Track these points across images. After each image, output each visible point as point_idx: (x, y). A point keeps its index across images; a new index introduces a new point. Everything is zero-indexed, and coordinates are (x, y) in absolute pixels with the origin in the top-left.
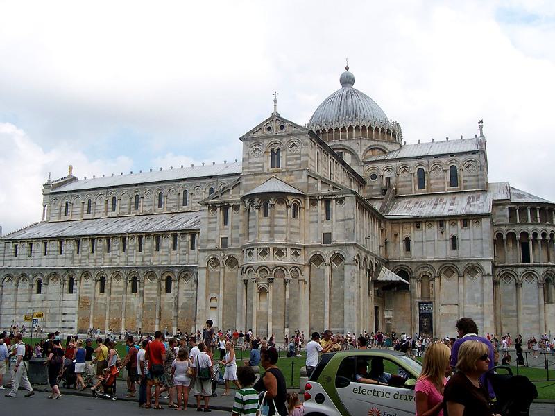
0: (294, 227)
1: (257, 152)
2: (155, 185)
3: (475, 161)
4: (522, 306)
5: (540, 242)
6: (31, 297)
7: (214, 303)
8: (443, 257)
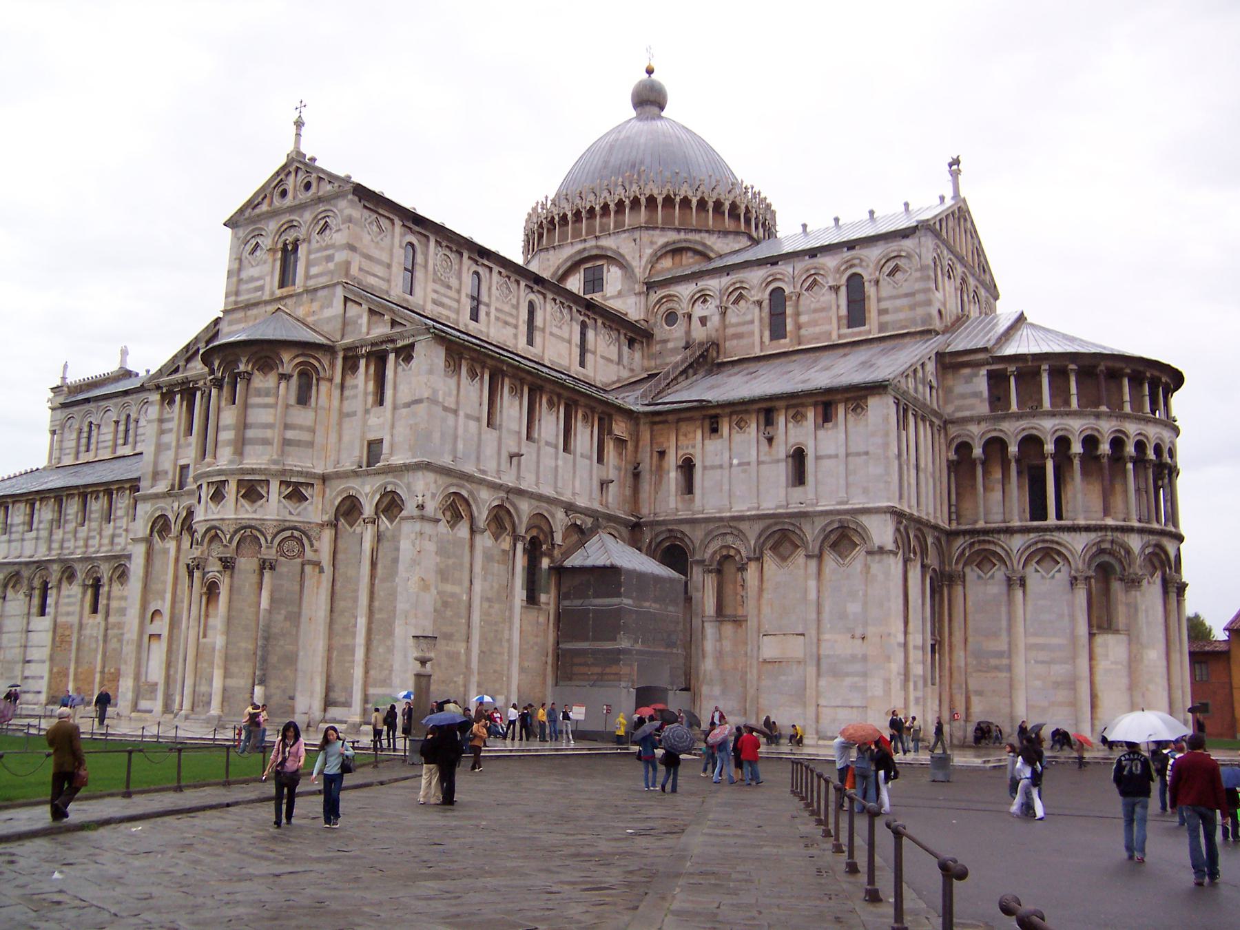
0: (301, 428)
1: (258, 253)
3: (909, 257)
4: (1021, 642)
5: (1077, 462)
8: (770, 504)
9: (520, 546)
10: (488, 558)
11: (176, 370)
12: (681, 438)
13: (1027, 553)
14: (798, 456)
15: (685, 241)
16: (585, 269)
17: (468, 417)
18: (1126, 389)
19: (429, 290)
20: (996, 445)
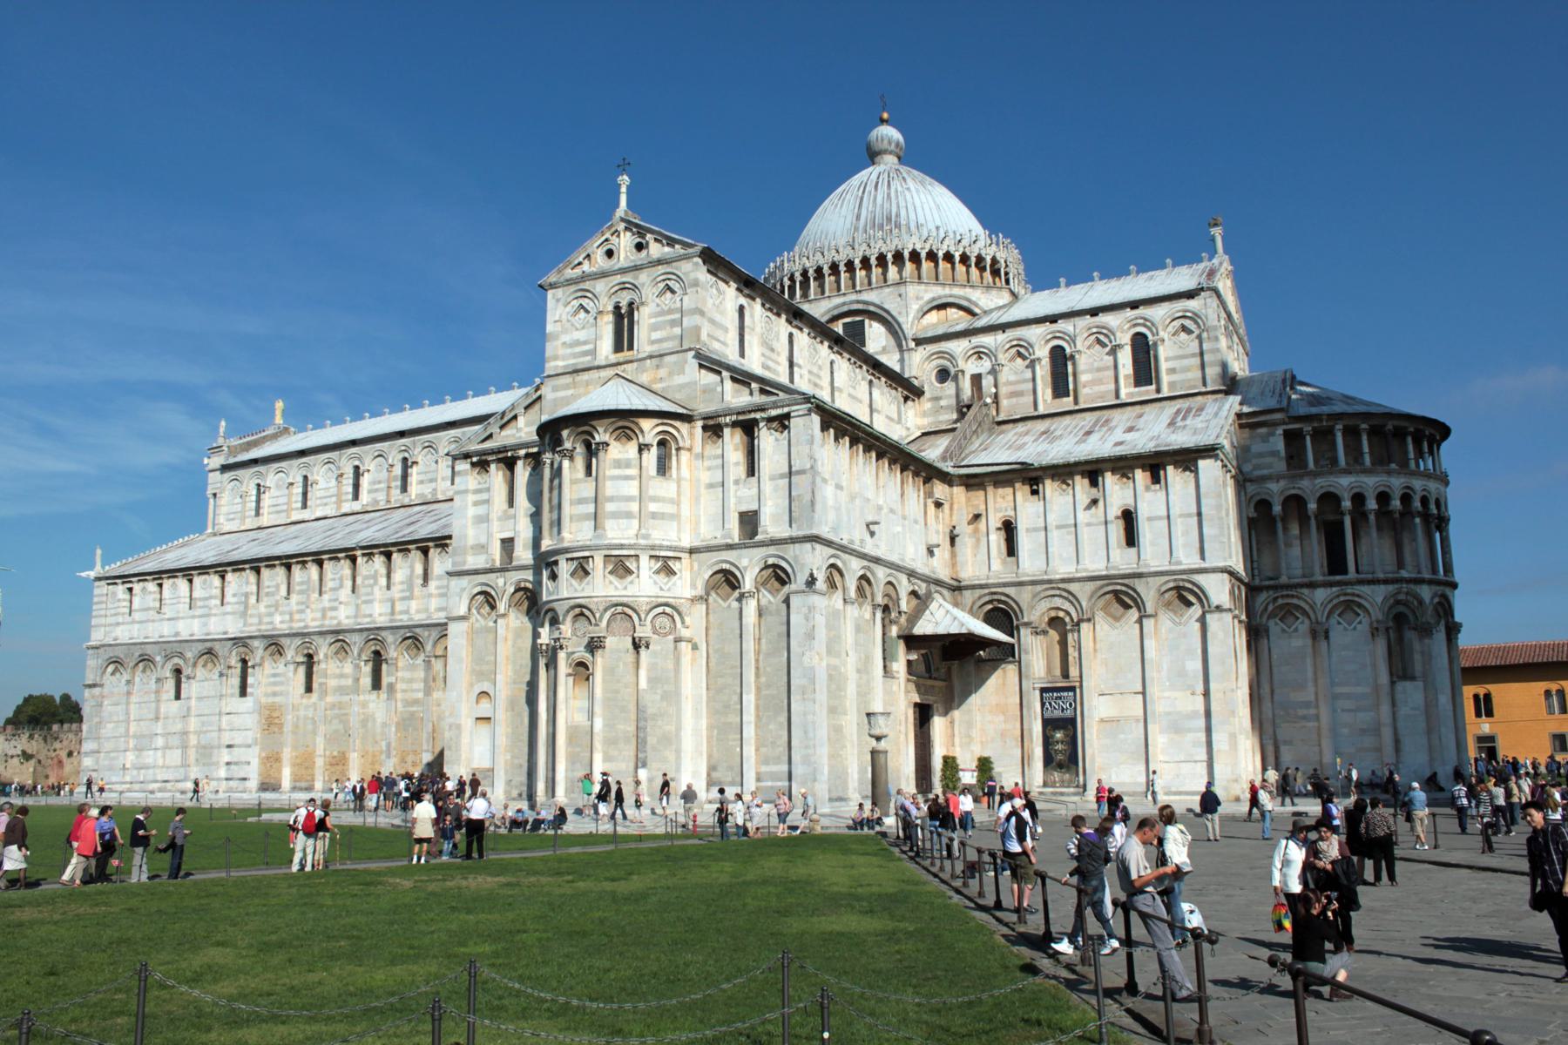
5: (1372, 517)
6: (157, 710)
7: (485, 708)
9: (879, 615)
10: (858, 629)
11: (490, 436)
13: (1330, 606)
14: (1129, 518)
16: (844, 324)
18: (1411, 447)
20: (1295, 503)
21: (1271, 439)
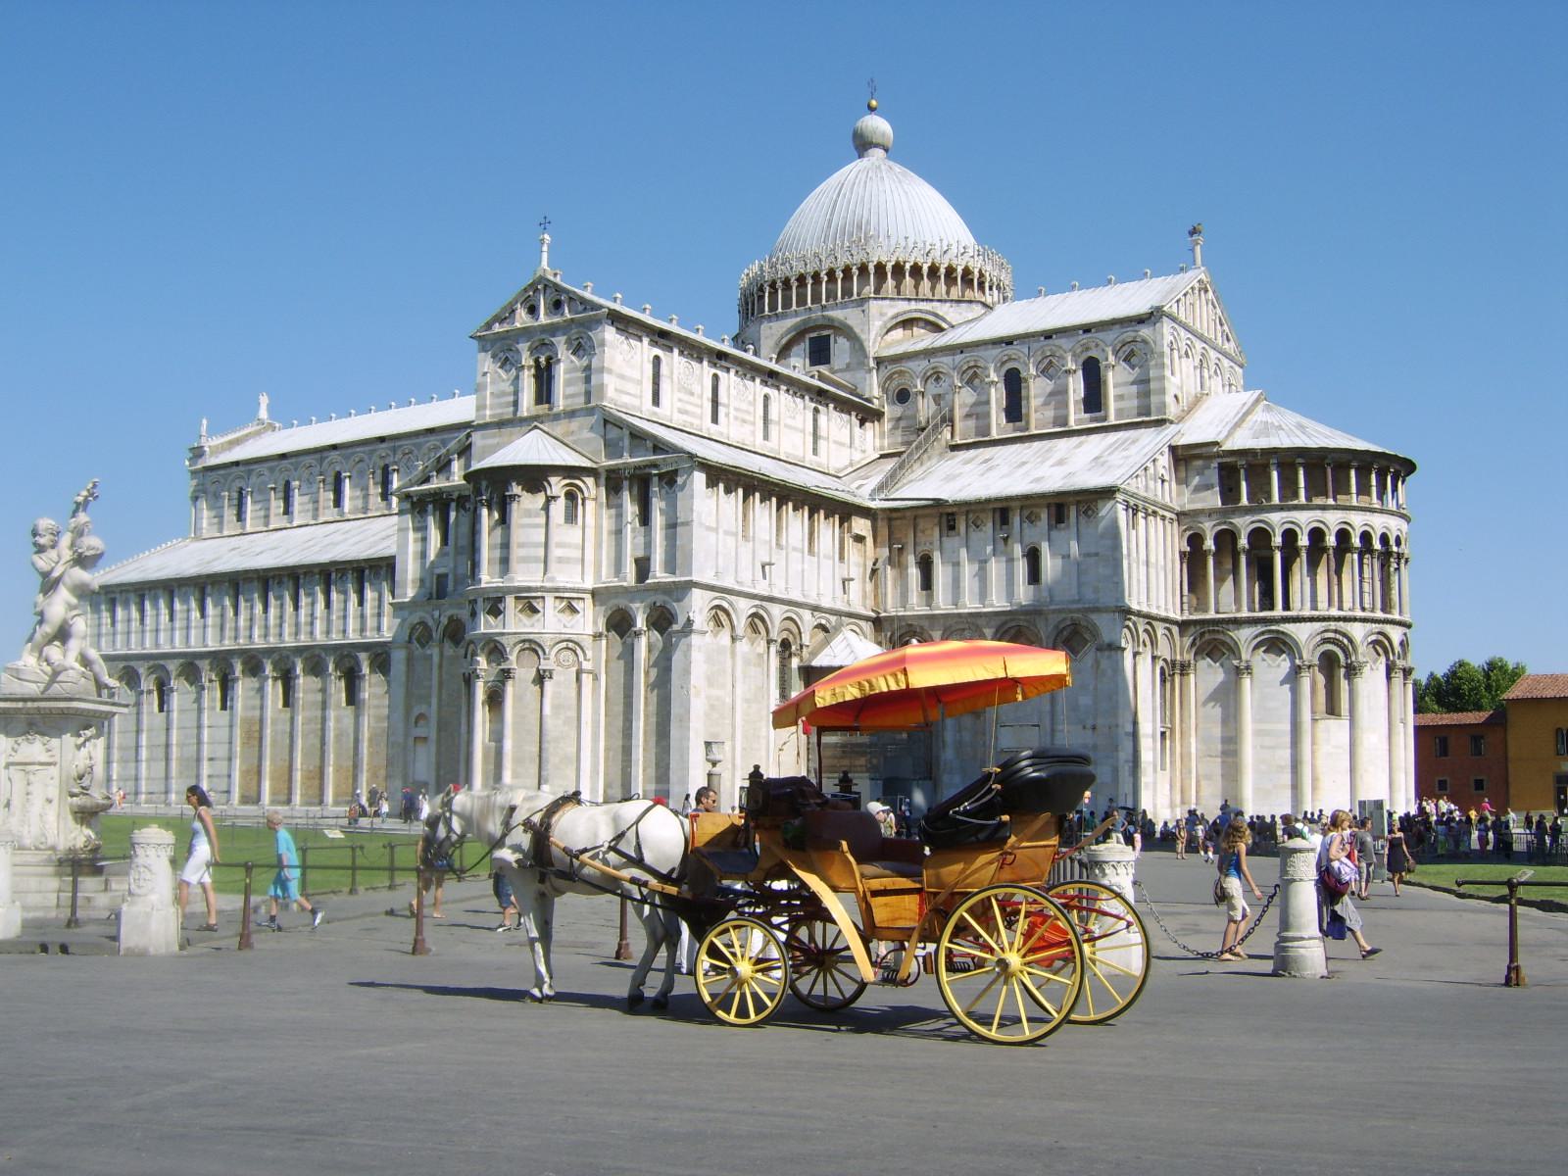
2: (421, 440)
9: (773, 649)
10: (747, 662)
12: (919, 534)
15: (916, 311)
16: (810, 339)
17: (727, 533)
19: (675, 400)
20: (1225, 539)
21: (1206, 472)
